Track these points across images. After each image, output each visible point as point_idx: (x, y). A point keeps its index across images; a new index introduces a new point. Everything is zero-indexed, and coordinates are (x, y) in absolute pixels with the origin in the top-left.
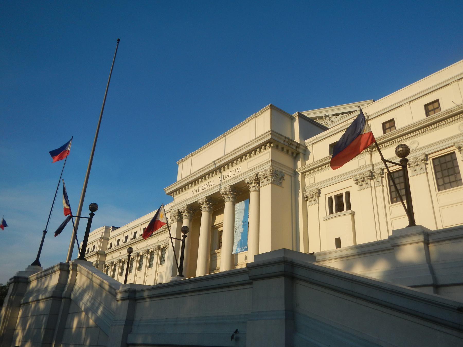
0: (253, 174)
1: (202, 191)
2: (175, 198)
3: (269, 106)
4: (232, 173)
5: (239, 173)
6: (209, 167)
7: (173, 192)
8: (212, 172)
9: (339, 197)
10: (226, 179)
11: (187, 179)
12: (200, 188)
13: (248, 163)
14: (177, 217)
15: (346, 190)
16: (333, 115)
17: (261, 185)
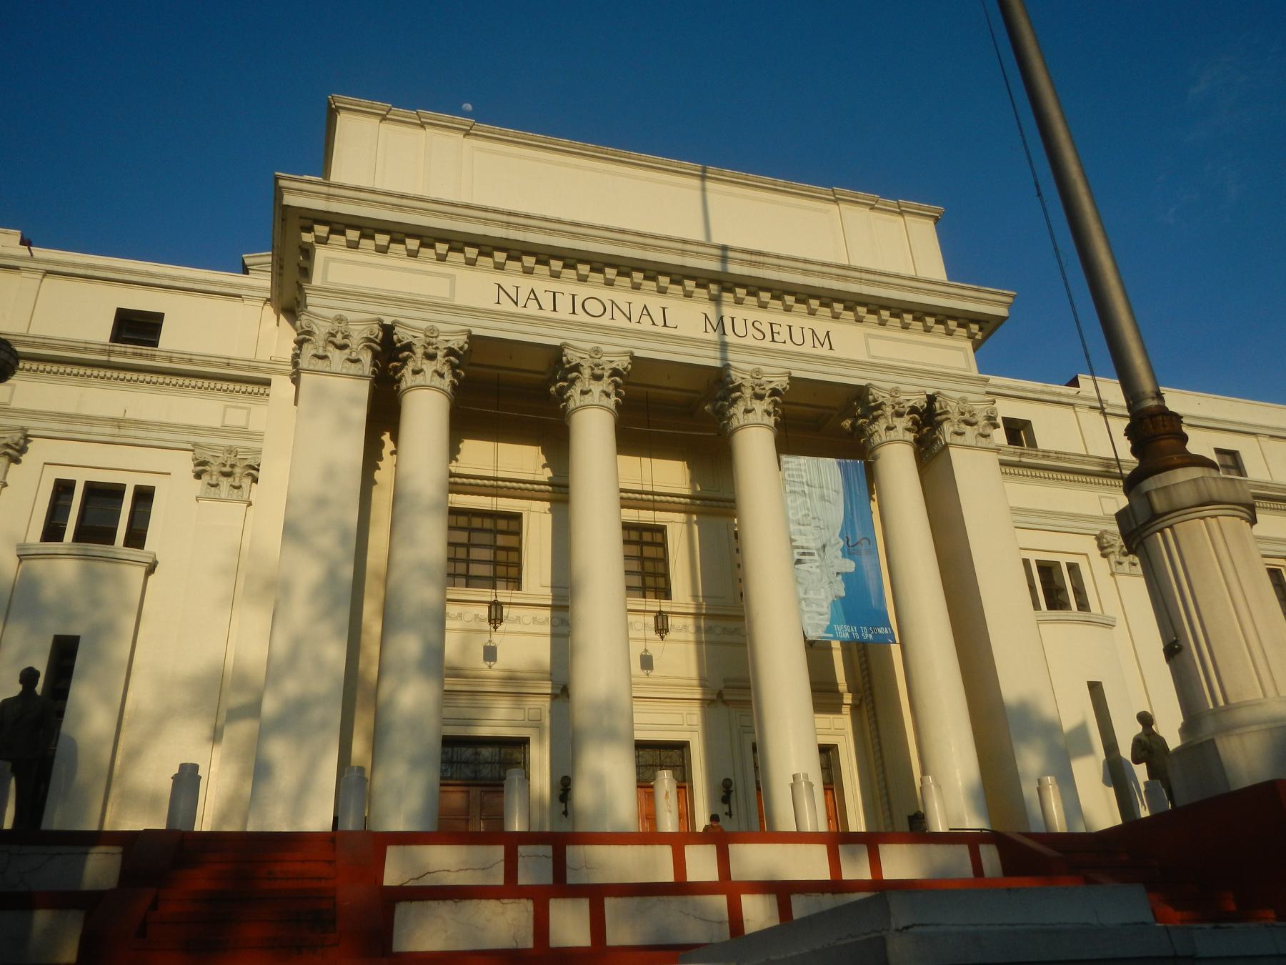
1: (581, 317)
2: (321, 253)
3: (937, 209)
7: (338, 224)
8: (679, 275)
9: (1048, 570)
10: (749, 341)
11: (508, 225)
12: (564, 303)
13: (868, 336)
14: (367, 358)
15: (1073, 559)
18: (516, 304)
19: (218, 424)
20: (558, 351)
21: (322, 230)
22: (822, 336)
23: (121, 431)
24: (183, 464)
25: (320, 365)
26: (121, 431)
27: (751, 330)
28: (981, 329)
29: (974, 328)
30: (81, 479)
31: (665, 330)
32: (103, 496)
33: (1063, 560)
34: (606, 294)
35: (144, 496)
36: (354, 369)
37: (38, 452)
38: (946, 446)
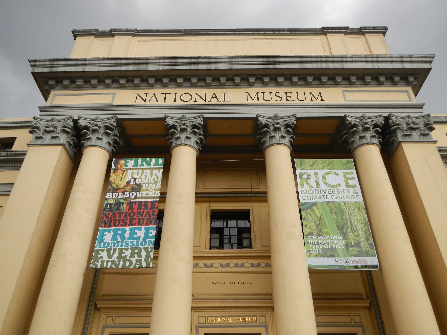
0: (375, 115)
1: (179, 102)
4: (294, 96)
6: (231, 63)
10: (273, 102)
18: (145, 101)
20: (164, 119)
21: (52, 82)
22: (316, 94)
25: (39, 142)
27: (274, 97)
28: (416, 79)
29: (411, 79)
31: (225, 103)
34: (193, 91)
36: (55, 141)
38: (400, 143)
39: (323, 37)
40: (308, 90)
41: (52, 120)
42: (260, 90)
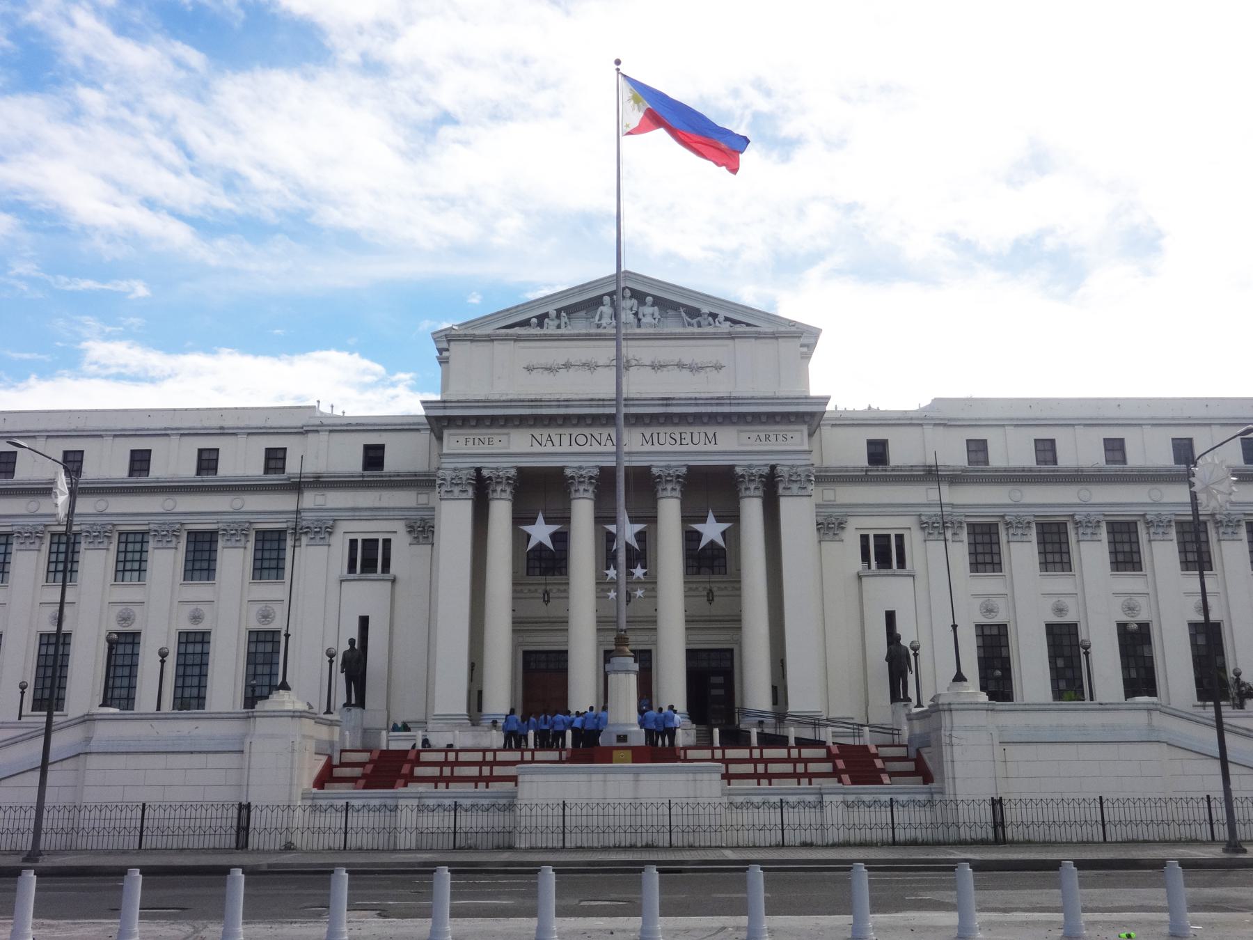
0: (761, 463)
1: (575, 448)
4: (688, 439)
5: (711, 447)
9: (882, 540)
11: (532, 407)
12: (566, 439)
16: (727, 319)
17: (781, 491)
19: (414, 504)
23: (375, 513)
24: (400, 527)
25: (449, 496)
26: (375, 513)
27: (669, 439)
30: (360, 537)
32: (370, 544)
33: (893, 534)
34: (587, 431)
35: (387, 542)
36: (464, 495)
37: (343, 526)
39: (729, 342)
40: (703, 429)
41: (455, 469)
42: (655, 430)
